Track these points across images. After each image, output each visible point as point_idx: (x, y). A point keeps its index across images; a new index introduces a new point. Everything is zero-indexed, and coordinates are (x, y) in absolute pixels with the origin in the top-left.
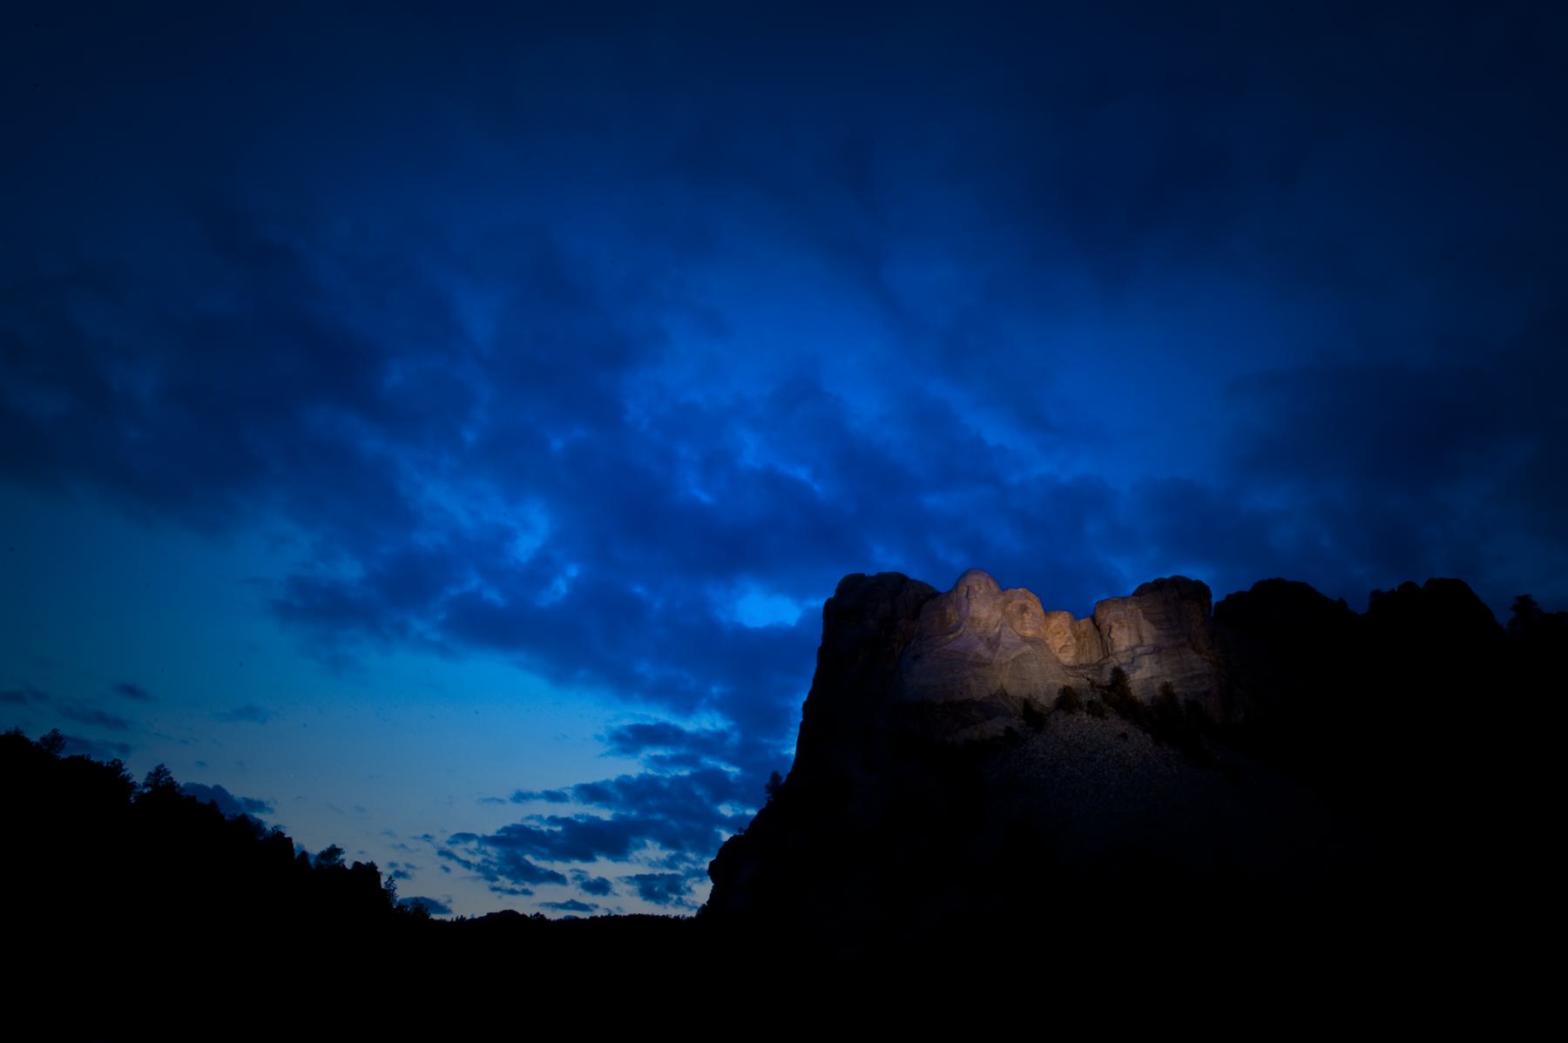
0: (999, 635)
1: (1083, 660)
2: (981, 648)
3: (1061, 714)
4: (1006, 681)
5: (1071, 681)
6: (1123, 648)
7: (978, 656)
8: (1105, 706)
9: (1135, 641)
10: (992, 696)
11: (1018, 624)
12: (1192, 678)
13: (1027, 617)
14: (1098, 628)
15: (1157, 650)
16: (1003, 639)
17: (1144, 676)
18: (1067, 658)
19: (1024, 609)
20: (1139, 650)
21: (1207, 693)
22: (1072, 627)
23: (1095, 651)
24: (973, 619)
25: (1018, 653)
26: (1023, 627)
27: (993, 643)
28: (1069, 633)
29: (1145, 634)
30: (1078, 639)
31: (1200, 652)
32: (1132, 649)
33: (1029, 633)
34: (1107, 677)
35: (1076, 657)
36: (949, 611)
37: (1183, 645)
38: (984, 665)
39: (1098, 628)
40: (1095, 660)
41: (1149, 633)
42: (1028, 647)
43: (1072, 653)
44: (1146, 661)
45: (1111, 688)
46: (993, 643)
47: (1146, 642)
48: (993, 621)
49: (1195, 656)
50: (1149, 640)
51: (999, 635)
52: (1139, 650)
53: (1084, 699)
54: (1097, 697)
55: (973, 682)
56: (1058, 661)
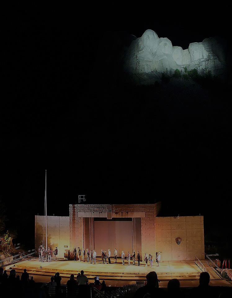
0: (156, 53)
9: (201, 57)
18: (179, 63)
19: (166, 44)
29: (204, 55)
32: (200, 59)
33: (167, 53)
40: (188, 64)
50: (205, 57)
51: (156, 53)
52: (202, 60)
55: (146, 67)
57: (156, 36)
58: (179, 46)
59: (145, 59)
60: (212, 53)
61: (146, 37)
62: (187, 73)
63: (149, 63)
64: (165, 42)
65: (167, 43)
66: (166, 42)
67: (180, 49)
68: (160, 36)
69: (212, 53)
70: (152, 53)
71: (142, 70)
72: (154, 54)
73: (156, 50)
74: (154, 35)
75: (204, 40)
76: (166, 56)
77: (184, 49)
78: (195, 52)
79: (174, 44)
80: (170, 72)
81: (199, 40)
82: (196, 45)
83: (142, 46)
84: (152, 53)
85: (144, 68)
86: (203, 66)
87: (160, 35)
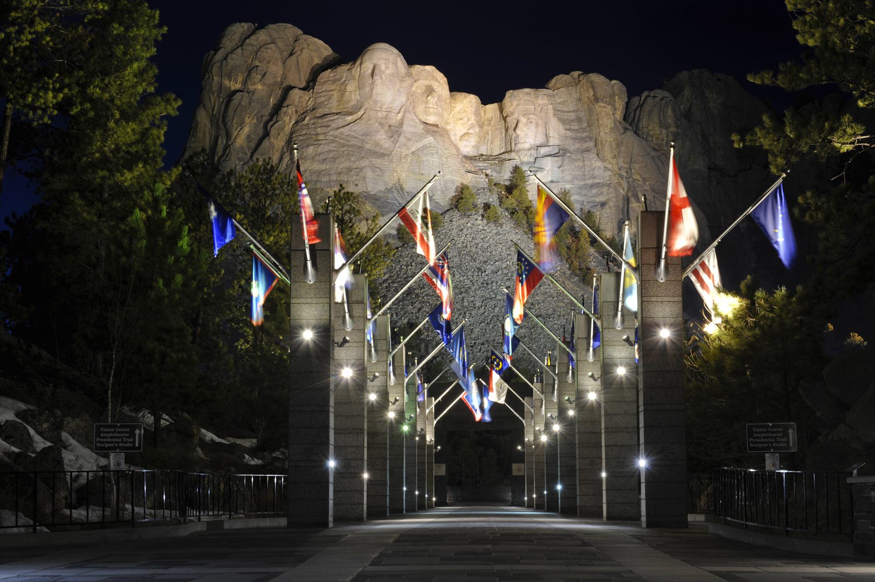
1: (484, 151)
2: (382, 138)
3: (456, 214)
4: (404, 175)
5: (469, 179)
6: (527, 146)
7: (377, 144)
8: (500, 210)
9: (540, 139)
10: (389, 190)
11: (420, 108)
12: (592, 186)
13: (432, 100)
14: (505, 119)
15: (560, 153)
16: (405, 128)
17: (546, 177)
18: (468, 147)
19: (430, 91)
20: (543, 151)
21: (603, 204)
22: (477, 113)
23: (497, 143)
24: (375, 102)
25: (420, 145)
26: (426, 113)
27: (395, 131)
28: (473, 120)
29: (552, 133)
30: (481, 126)
31: (603, 160)
33: (432, 119)
34: (505, 177)
35: (476, 147)
36: (349, 88)
37: (587, 150)
38: (383, 155)
39: (505, 119)
40: (496, 153)
41: (557, 133)
42: (430, 139)
43: (473, 141)
44: (549, 164)
45: (510, 189)
46: (395, 131)
48: (397, 105)
49: (599, 164)
50: (554, 140)
51: (401, 124)
52: (543, 151)
53: (480, 201)
54: (493, 199)
55: (369, 174)
56: (458, 149)
57: (401, 61)
59: (368, 146)
61: (370, 71)
63: (378, 162)
64: (427, 83)
68: (411, 60)
71: (357, 185)
73: (400, 116)
74: (395, 64)
75: (554, 80)
77: (485, 102)
78: (523, 120)
79: (455, 87)
82: (526, 98)
85: (364, 178)
87: (412, 58)
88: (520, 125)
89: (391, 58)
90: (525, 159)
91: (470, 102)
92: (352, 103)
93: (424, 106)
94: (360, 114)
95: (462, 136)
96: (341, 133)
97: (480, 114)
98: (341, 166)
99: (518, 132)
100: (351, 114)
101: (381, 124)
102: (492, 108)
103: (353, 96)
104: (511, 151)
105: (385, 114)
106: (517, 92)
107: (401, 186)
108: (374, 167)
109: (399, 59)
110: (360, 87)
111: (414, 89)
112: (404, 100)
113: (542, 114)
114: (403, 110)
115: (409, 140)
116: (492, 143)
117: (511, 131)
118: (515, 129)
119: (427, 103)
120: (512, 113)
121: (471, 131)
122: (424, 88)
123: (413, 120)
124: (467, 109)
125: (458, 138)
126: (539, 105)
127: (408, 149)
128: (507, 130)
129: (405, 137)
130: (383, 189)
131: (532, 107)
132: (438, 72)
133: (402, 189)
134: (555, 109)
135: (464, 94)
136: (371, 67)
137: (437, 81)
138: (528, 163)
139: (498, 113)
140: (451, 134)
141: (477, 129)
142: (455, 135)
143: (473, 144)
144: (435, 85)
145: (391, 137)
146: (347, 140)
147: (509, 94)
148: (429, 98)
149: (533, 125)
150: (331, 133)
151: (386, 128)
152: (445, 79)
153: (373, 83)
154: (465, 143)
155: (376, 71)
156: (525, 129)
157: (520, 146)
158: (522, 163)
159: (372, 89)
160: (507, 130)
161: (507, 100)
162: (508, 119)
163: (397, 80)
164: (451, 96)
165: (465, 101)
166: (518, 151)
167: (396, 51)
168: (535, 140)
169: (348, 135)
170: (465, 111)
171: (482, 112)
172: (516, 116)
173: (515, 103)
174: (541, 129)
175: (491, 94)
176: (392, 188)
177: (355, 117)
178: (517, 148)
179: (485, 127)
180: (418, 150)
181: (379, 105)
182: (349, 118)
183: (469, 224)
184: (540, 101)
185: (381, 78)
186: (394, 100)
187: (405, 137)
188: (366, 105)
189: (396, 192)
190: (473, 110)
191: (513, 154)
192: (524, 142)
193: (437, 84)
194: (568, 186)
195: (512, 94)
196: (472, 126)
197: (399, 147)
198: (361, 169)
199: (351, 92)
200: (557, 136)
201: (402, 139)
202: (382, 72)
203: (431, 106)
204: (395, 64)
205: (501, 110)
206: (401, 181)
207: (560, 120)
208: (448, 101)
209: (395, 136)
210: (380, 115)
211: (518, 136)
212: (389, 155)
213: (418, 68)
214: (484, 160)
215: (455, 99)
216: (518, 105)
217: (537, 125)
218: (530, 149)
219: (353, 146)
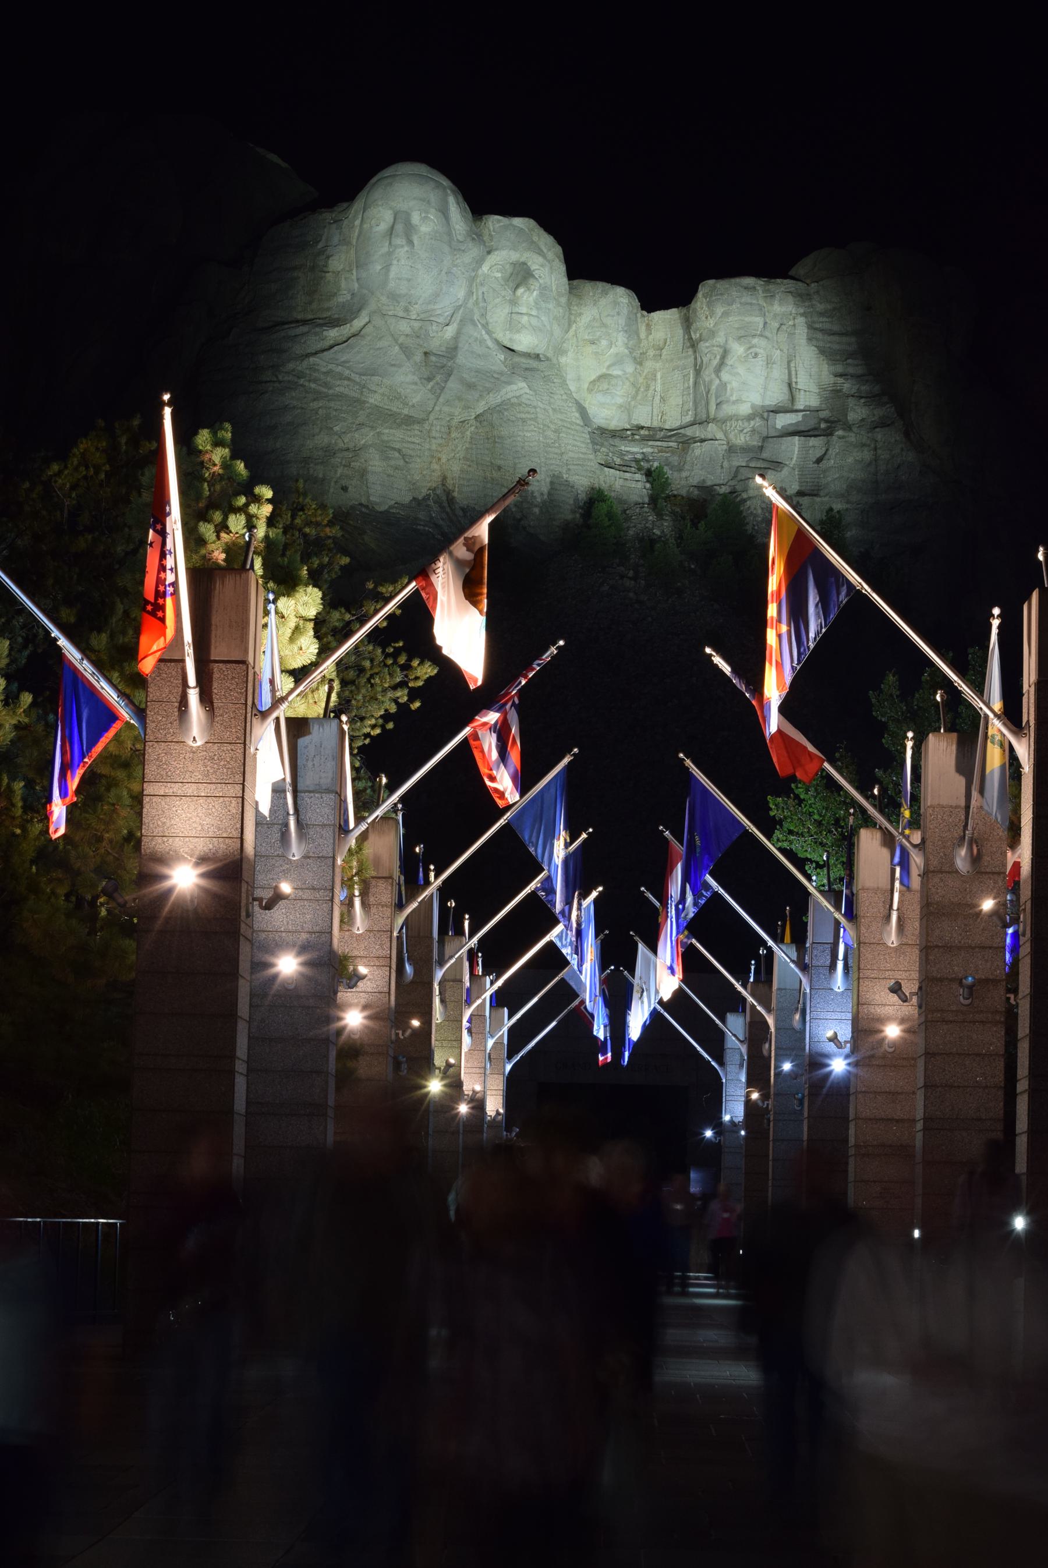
0: (453, 350)
1: (643, 417)
6: (745, 409)
9: (776, 395)
11: (498, 315)
13: (527, 297)
14: (693, 345)
16: (461, 359)
18: (607, 411)
19: (521, 276)
22: (631, 330)
24: (394, 297)
25: (494, 399)
26: (512, 325)
28: (620, 344)
30: (639, 362)
33: (524, 342)
35: (627, 409)
38: (409, 421)
39: (693, 345)
40: (673, 421)
43: (620, 394)
47: (800, 405)
48: (444, 306)
50: (809, 397)
51: (453, 350)
52: (782, 421)
55: (375, 464)
58: (615, 279)
59: (373, 400)
60: (860, 370)
61: (383, 227)
62: (664, 528)
64: (515, 256)
65: (535, 263)
66: (523, 246)
67: (625, 311)
69: (860, 370)
70: (426, 354)
71: (345, 489)
72: (439, 365)
73: (450, 332)
74: (444, 212)
76: (523, 385)
77: (650, 303)
78: (738, 349)
80: (551, 503)
81: (763, 259)
82: (747, 298)
83: (346, 288)
84: (426, 354)
85: (363, 473)
86: (785, 471)
87: (484, 199)
88: (730, 361)
89: (434, 196)
90: (741, 440)
91: (616, 303)
92: (341, 299)
93: (507, 311)
94: (357, 324)
95: (593, 382)
96: (313, 368)
97: (637, 334)
98: (310, 444)
99: (725, 376)
100: (335, 323)
101: (406, 350)
102: (665, 321)
103: (343, 284)
104: (707, 421)
105: (417, 325)
106: (721, 285)
107: (448, 493)
108: (385, 449)
109: (451, 200)
110: (359, 265)
111: (485, 268)
112: (461, 294)
113: (783, 337)
114: (458, 317)
115: (471, 386)
116: (663, 400)
117: (708, 374)
118: (718, 370)
119: (514, 302)
120: (713, 333)
121: (616, 372)
122: (509, 269)
123: (482, 342)
124: (608, 321)
125: (586, 386)
126: (775, 315)
127: (467, 407)
128: (698, 372)
129: (462, 381)
130: (407, 499)
131: (759, 321)
132: (542, 232)
133: (451, 500)
134: (810, 327)
135: (600, 285)
136: (388, 216)
137: (540, 253)
138: (746, 449)
139: (680, 332)
140: (570, 376)
141: (630, 368)
142: (579, 379)
143: (620, 401)
144: (535, 263)
145: (429, 379)
146: (326, 385)
147: (705, 288)
148: (520, 291)
149: (760, 362)
150: (291, 366)
151: (418, 357)
152: (559, 249)
153: (390, 254)
154: (600, 398)
155: (400, 227)
156: (741, 370)
157: (728, 410)
158: (731, 449)
159: (387, 268)
160: (698, 372)
161: (700, 302)
162: (703, 345)
163: (446, 249)
164: (571, 288)
165: (603, 302)
166: (724, 422)
167: (445, 182)
168: (763, 396)
169: (327, 373)
170: (604, 325)
171: (643, 329)
172: (720, 339)
173: (719, 310)
174: (778, 373)
175: (663, 287)
176: (427, 498)
177: (346, 330)
178: (721, 415)
179: (649, 365)
180: (491, 410)
181: (403, 304)
182: (333, 334)
183: (606, 588)
184: (777, 308)
185: (410, 242)
186: (436, 295)
187: (462, 381)
188: (372, 305)
189: (435, 508)
190: (622, 321)
191: (712, 427)
192: (738, 401)
193: (541, 259)
194: (837, 506)
195: (714, 287)
196: (618, 361)
197: (447, 402)
198: (357, 451)
199: (337, 274)
200: (815, 389)
201: (453, 384)
202: (409, 229)
203: (524, 310)
204: (444, 212)
205: (687, 323)
206: (450, 482)
207: (822, 351)
208: (563, 300)
209: (438, 378)
210: (404, 327)
211: (723, 386)
212: (420, 422)
213: (494, 222)
214: (645, 439)
215: (580, 297)
216: (726, 314)
217: (769, 362)
218: (750, 418)
219: (340, 396)
